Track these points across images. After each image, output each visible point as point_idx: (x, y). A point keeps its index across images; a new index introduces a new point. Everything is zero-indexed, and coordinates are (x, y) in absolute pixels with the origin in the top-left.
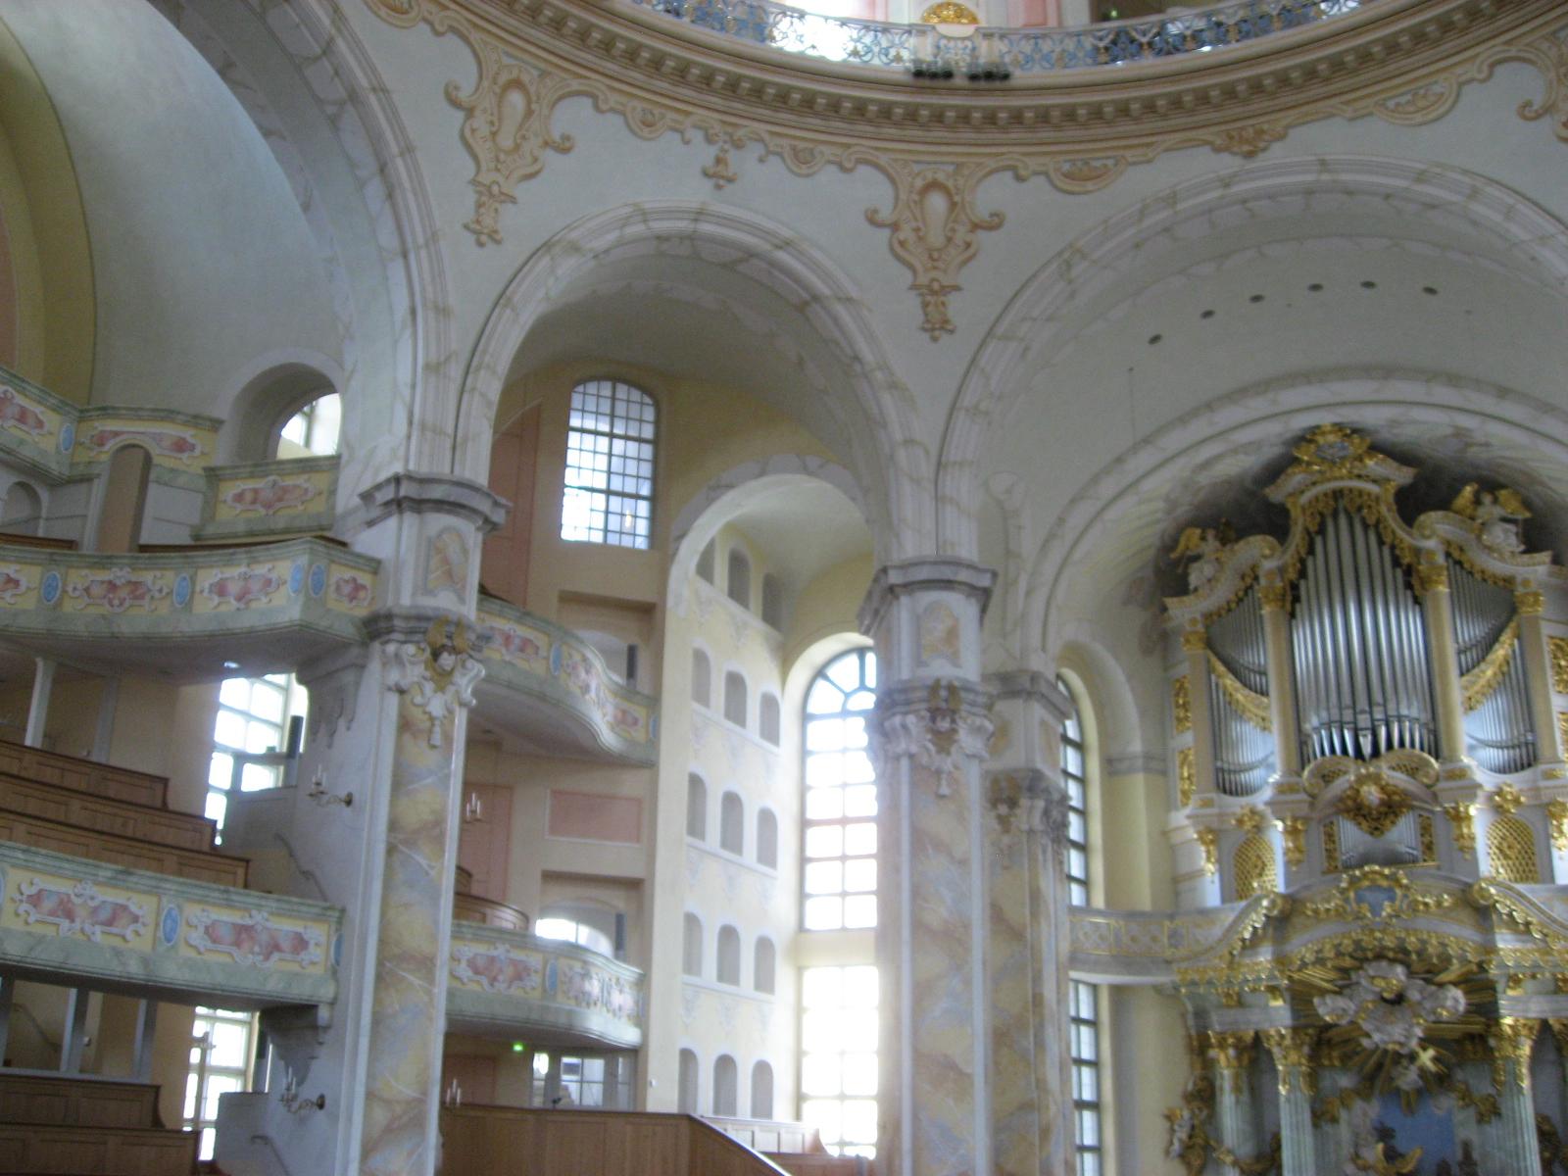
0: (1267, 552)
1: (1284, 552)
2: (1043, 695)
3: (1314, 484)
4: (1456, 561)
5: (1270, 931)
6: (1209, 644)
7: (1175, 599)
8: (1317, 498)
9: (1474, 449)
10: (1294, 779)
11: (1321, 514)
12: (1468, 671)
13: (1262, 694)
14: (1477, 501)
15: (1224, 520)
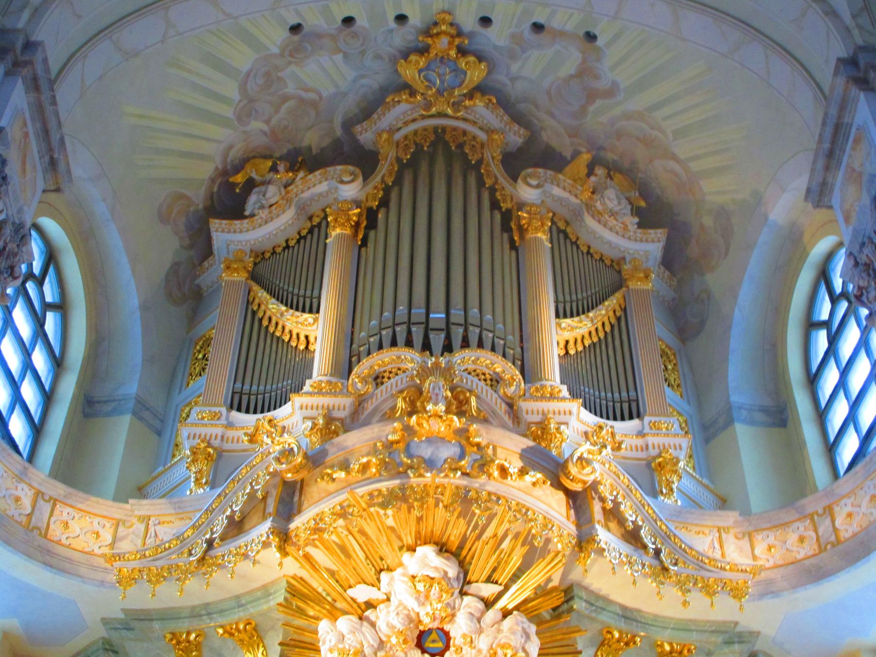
0: (347, 178)
1: (367, 184)
2: (35, 79)
3: (414, 120)
4: (562, 235)
5: (271, 507)
6: (254, 277)
7: (224, 222)
8: (416, 133)
9: (599, 103)
10: (334, 380)
11: (416, 144)
12: (565, 316)
13: (311, 312)
14: (590, 173)
15: (300, 160)
